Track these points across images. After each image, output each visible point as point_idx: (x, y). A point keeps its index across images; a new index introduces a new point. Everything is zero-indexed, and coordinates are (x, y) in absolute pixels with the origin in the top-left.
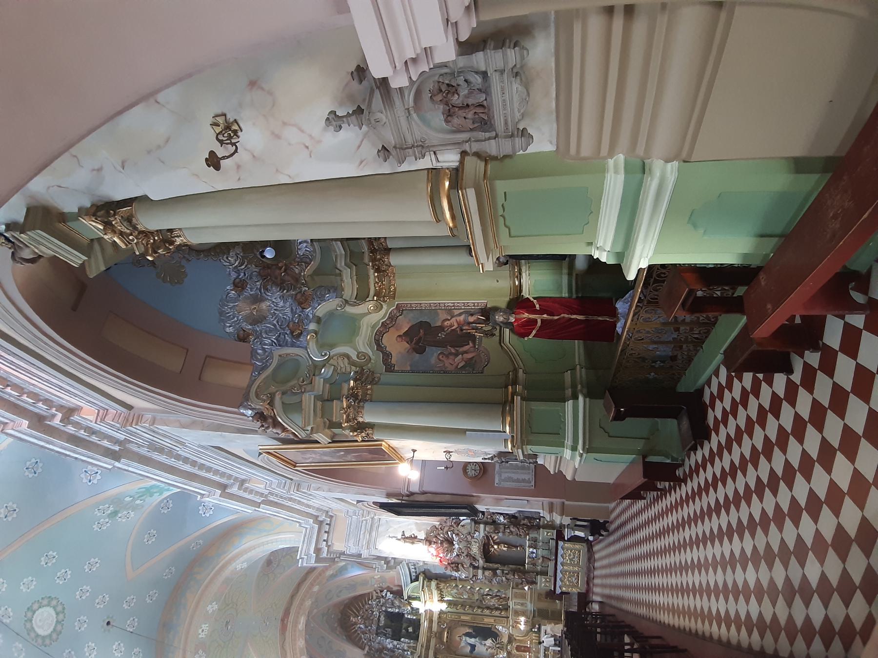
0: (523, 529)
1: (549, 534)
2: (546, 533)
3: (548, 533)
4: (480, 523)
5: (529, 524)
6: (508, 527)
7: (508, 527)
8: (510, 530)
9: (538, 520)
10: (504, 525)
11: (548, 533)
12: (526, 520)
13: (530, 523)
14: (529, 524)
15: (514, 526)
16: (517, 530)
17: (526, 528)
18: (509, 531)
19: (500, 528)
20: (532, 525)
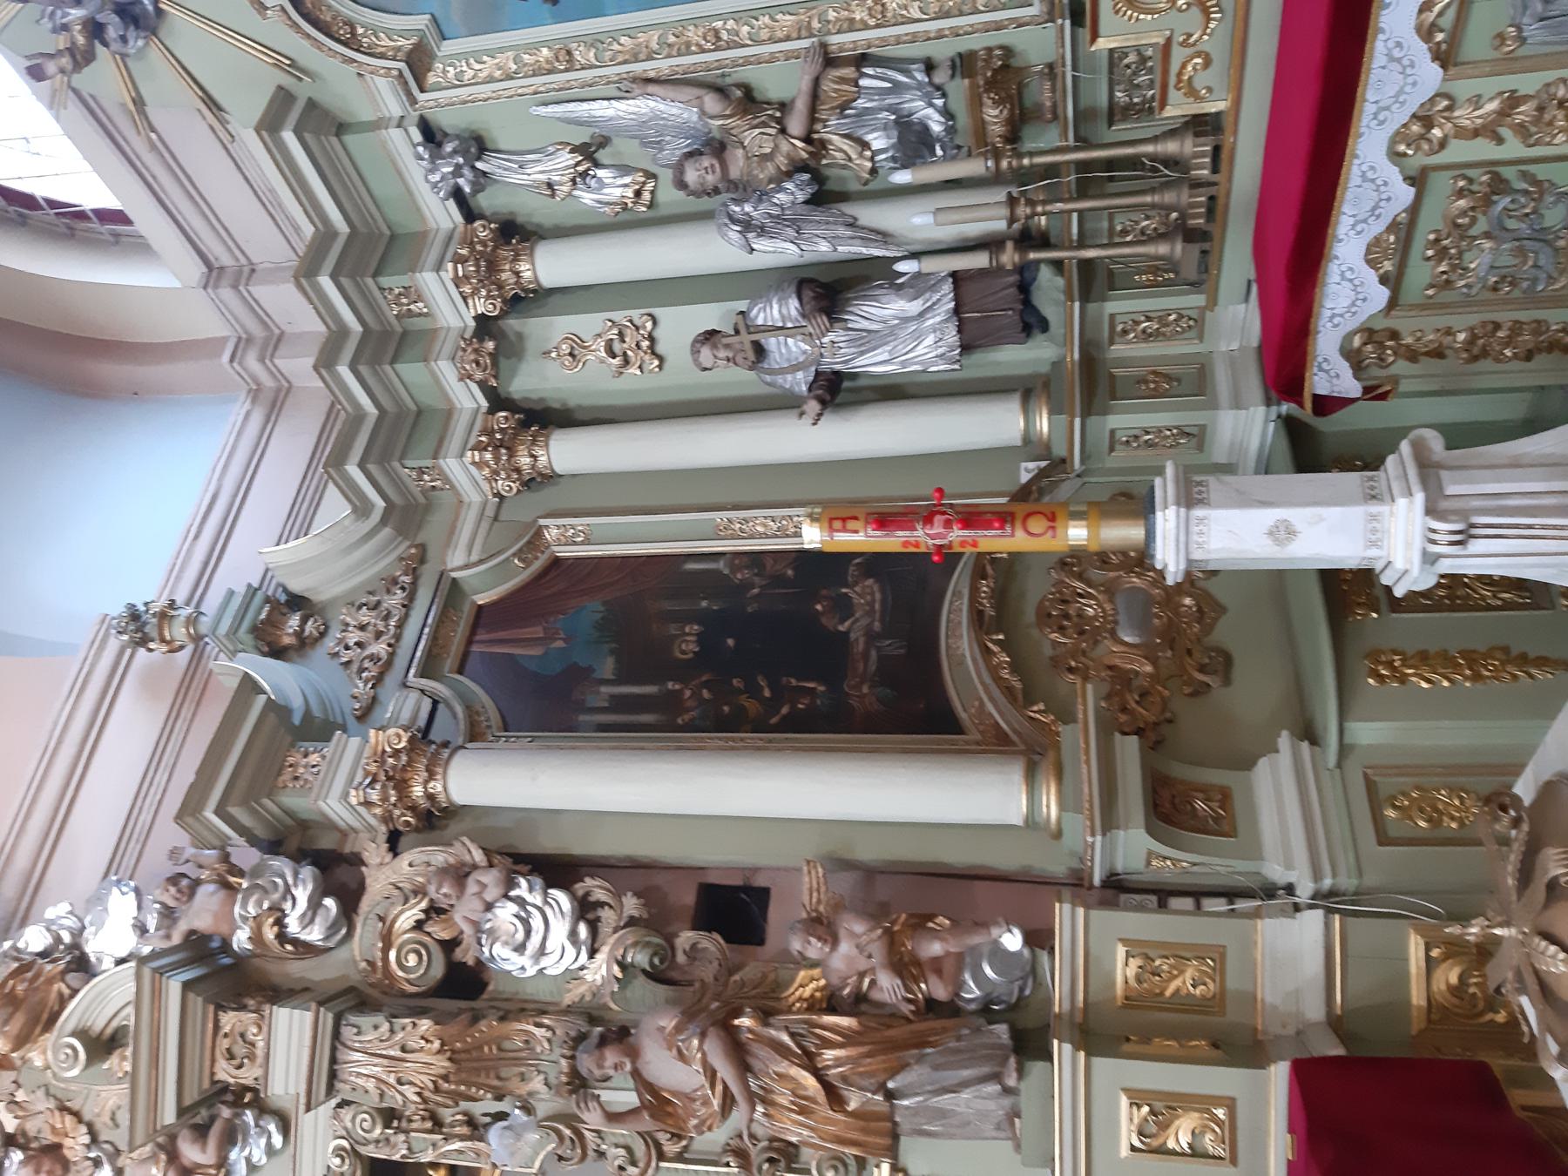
0: (809, 1061)
1: (1180, 1135)
2: (1126, 1123)
3: (1164, 1107)
4: (279, 994)
5: (888, 987)
6: (620, 1036)
7: (620, 1036)
8: (643, 1084)
9: (1013, 941)
10: (591, 1013)
11: (1164, 1107)
12: (854, 927)
13: (906, 967)
14: (888, 987)
15: (690, 1015)
16: (726, 1072)
17: (849, 1038)
18: (626, 1098)
19: (525, 1057)
20: (931, 1007)
